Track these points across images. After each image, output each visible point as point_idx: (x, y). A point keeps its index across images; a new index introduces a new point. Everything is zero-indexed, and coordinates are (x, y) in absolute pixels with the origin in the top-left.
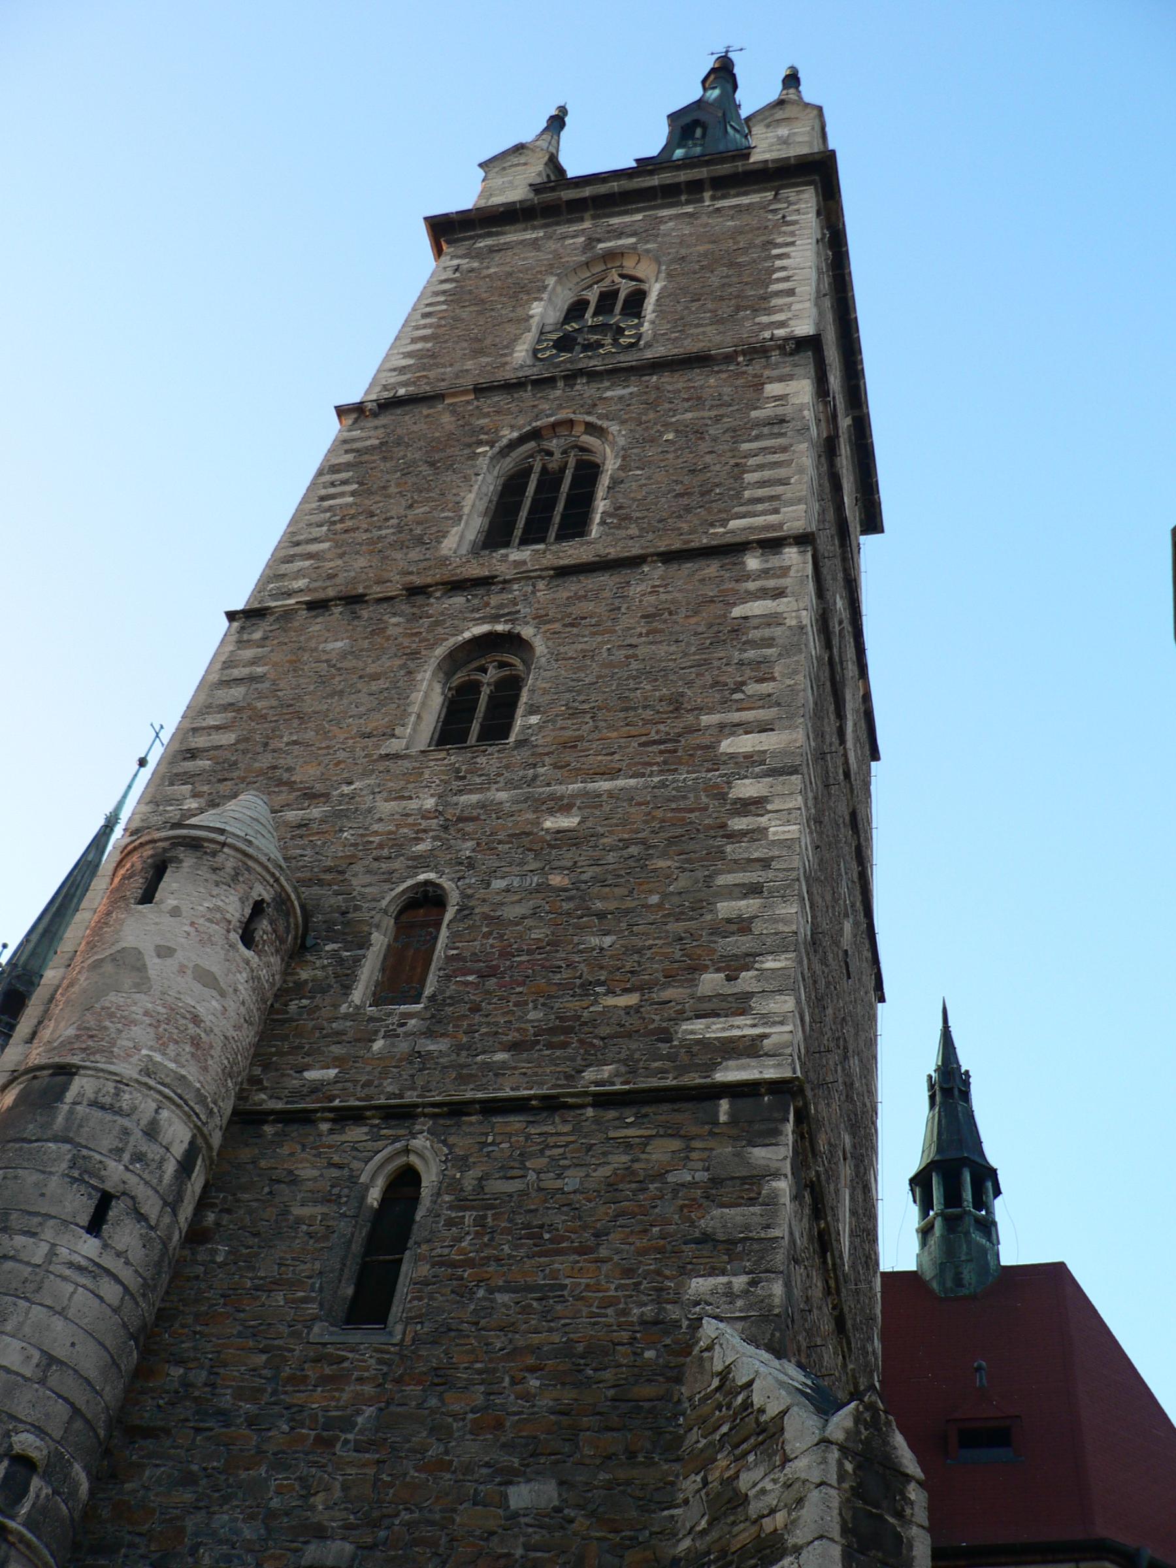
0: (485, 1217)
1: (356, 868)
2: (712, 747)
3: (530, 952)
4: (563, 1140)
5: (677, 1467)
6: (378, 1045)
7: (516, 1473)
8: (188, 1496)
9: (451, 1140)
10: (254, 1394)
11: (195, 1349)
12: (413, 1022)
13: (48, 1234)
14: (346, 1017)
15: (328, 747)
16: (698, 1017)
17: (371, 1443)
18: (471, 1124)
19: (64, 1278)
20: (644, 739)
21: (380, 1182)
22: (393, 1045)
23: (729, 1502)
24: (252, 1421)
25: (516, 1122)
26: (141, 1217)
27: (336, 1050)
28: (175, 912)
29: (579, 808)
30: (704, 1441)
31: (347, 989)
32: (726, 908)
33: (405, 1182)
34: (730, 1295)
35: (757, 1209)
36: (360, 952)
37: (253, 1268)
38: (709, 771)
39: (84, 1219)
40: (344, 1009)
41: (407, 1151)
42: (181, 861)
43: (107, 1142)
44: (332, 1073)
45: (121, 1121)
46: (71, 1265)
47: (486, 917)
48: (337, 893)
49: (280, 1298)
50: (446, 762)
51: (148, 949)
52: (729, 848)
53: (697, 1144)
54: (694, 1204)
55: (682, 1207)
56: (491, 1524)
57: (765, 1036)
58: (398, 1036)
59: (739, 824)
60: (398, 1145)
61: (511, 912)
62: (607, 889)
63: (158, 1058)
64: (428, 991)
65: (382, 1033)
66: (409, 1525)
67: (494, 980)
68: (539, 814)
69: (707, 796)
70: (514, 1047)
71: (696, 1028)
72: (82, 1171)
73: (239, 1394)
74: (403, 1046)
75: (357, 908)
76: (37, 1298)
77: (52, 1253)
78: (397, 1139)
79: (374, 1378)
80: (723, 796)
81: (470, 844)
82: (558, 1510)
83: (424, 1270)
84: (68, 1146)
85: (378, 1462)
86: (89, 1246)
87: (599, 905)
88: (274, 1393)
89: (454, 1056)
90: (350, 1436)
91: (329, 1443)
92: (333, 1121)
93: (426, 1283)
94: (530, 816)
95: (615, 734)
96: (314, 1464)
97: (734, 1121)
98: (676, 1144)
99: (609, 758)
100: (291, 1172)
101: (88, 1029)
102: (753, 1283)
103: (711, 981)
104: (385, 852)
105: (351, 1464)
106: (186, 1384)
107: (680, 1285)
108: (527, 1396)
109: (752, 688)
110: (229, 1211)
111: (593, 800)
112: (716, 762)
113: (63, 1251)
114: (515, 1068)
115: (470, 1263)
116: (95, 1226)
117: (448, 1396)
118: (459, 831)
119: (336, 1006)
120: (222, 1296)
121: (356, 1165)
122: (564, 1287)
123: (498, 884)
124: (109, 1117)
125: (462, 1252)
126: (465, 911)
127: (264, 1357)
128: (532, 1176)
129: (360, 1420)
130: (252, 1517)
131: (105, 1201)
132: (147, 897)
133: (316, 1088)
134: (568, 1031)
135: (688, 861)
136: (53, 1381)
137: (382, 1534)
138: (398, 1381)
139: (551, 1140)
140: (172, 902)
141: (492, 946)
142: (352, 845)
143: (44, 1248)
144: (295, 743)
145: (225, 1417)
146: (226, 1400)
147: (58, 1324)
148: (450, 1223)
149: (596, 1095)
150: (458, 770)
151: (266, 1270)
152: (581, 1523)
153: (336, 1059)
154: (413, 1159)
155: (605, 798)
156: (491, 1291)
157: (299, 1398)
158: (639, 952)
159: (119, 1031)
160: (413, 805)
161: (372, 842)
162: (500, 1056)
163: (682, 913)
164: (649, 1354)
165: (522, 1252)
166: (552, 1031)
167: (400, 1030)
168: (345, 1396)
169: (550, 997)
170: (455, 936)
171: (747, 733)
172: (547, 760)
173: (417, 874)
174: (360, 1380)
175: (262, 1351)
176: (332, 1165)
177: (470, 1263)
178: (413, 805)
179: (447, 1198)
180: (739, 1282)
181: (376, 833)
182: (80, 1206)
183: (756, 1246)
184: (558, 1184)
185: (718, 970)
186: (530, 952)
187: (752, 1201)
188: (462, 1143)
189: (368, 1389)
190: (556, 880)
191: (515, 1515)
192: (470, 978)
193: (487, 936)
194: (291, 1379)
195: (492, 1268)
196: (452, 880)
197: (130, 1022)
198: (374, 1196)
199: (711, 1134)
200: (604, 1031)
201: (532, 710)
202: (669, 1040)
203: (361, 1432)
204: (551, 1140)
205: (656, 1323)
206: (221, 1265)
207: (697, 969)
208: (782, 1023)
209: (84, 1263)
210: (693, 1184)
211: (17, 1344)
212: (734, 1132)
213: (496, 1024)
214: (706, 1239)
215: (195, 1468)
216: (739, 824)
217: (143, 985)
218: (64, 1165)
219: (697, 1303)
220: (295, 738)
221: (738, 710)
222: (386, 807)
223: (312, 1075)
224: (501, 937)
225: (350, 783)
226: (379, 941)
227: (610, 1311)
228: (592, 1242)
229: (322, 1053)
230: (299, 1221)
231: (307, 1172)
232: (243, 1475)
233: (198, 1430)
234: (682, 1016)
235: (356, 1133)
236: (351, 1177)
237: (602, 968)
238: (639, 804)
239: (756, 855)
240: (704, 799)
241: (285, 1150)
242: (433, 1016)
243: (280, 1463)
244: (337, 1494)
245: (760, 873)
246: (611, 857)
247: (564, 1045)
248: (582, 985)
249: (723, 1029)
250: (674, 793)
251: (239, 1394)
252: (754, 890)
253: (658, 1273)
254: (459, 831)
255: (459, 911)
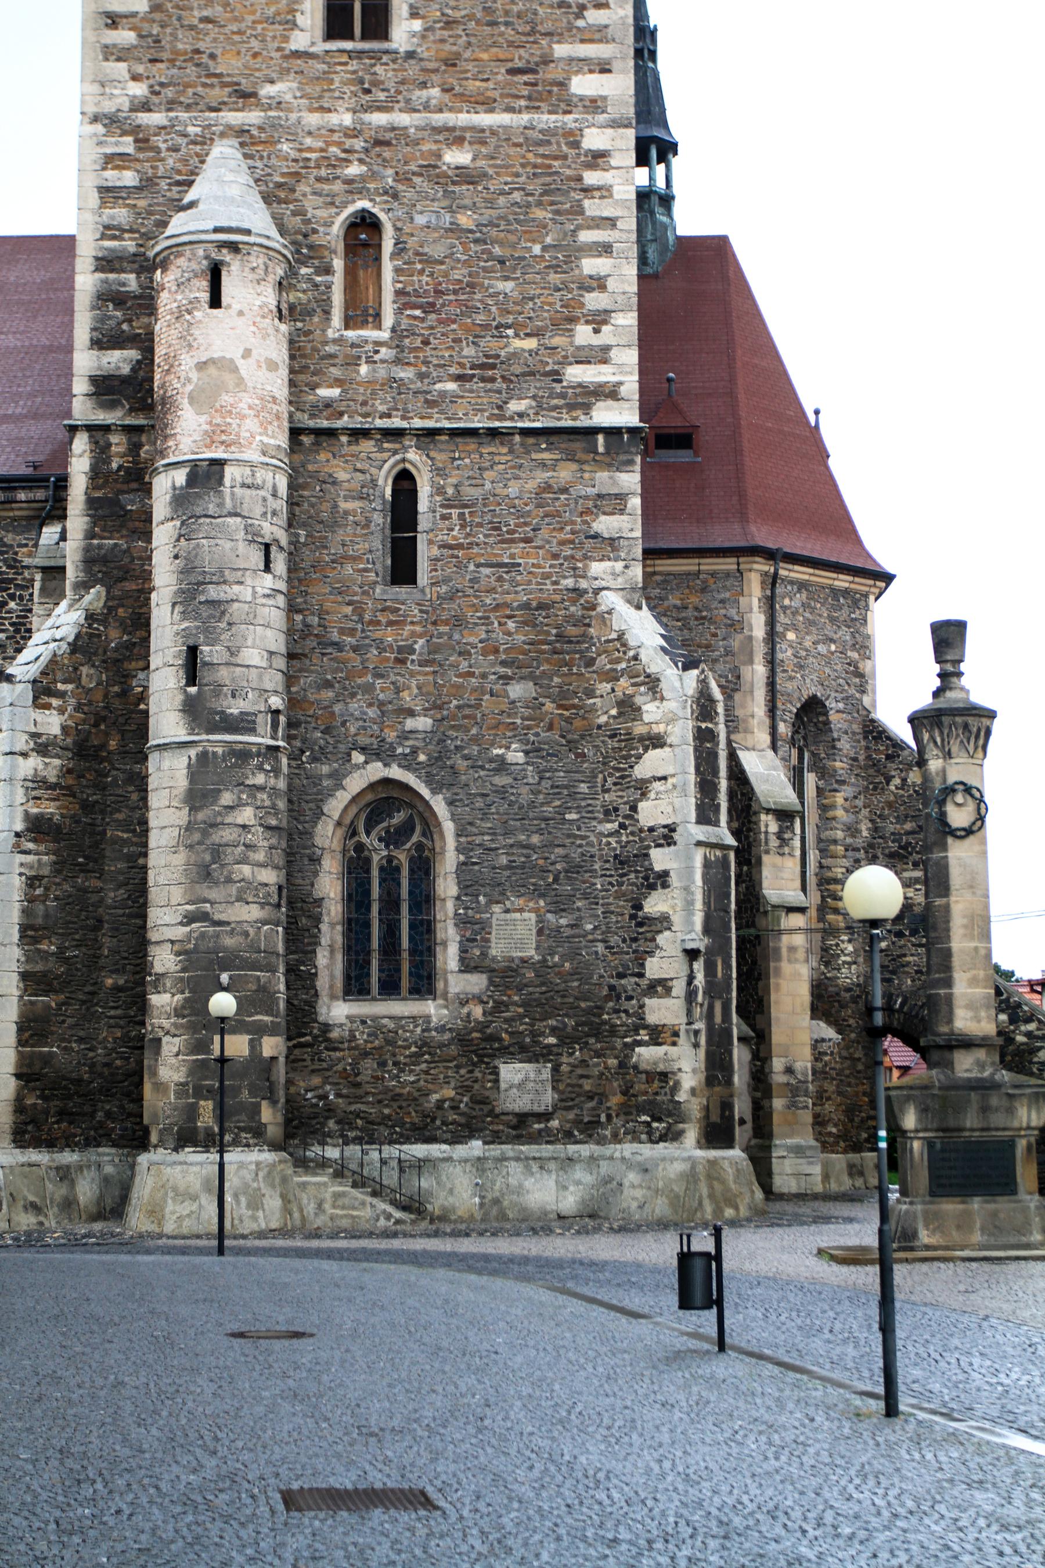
0: (463, 514)
1: (303, 188)
2: (563, 85)
3: (455, 292)
4: (503, 459)
5: (595, 676)
6: (364, 369)
7: (511, 678)
8: (330, 694)
9: (432, 454)
10: (352, 632)
11: (305, 602)
12: (383, 350)
13: (249, 581)
14: (335, 341)
15: (240, 33)
16: (577, 362)
17: (427, 661)
18: (442, 442)
19: (263, 605)
20: (510, 65)
21: (390, 482)
22: (374, 371)
23: (628, 708)
24: (355, 649)
25: (471, 444)
26: (281, 548)
27: (335, 372)
28: (241, 313)
29: (470, 143)
30: (608, 666)
31: (327, 313)
32: (590, 266)
33: (405, 480)
34: (615, 575)
35: (625, 517)
36: (328, 278)
37: (326, 547)
38: (566, 112)
39: (262, 566)
40: (331, 334)
41: (404, 460)
42: (229, 265)
43: (258, 511)
44: (335, 392)
45: (262, 493)
46: (264, 596)
47: (418, 254)
48: (294, 214)
49: (349, 569)
50: (349, 68)
51: (234, 353)
52: (587, 203)
53: (586, 467)
54: (587, 512)
55: (582, 513)
56: (504, 707)
57: (621, 383)
58: (375, 362)
59: (591, 178)
60: (398, 457)
61: (437, 251)
62: (502, 235)
63: (266, 440)
64: (388, 319)
65: (364, 359)
66: (458, 707)
67: (433, 316)
68: (439, 146)
69: (566, 144)
70: (459, 378)
71: (576, 374)
72: (253, 535)
73: (342, 631)
74: (382, 372)
75: (315, 231)
76: (255, 622)
77: (254, 593)
78: (395, 452)
79: (420, 622)
80: (576, 145)
81: (390, 172)
82: (536, 699)
83: (435, 551)
84: (239, 519)
85: (434, 672)
86: (268, 581)
87: (497, 250)
88: (363, 631)
89: (419, 384)
90: (414, 657)
91: (402, 662)
92: (350, 435)
93: (437, 560)
94: (434, 147)
95: (485, 56)
96: (399, 674)
97: (608, 452)
98: (574, 466)
99: (484, 84)
100: (330, 475)
101: (218, 425)
102: (626, 567)
103: (583, 334)
104: (323, 172)
105: (419, 673)
106: (307, 626)
107: (586, 566)
108: (509, 634)
109: (594, 17)
110: (298, 504)
111: (479, 136)
112: (568, 104)
113: (258, 589)
114: (462, 397)
115: (460, 547)
116: (267, 568)
117: (465, 632)
118: (379, 156)
119: (324, 331)
120: (313, 566)
121: (373, 471)
122: (519, 565)
123: (420, 220)
124: (254, 492)
125: (455, 538)
126: (400, 249)
127: (350, 608)
128: (488, 486)
129: (416, 647)
130: (370, 705)
131: (267, 546)
132: (215, 302)
133: (328, 404)
134: (493, 367)
135: (557, 212)
136: (274, 666)
137: (445, 713)
138: (434, 623)
139: (497, 459)
140: (236, 307)
141: (427, 284)
142: (294, 160)
143: (250, 589)
144: (206, 20)
145: (338, 646)
146: (335, 636)
147: (269, 633)
148: (444, 517)
149: (521, 429)
150: (361, 82)
151: (335, 549)
152: (549, 706)
153: (337, 380)
154: (408, 466)
155: (487, 134)
156: (478, 566)
157: (378, 634)
158: (532, 299)
159: (239, 426)
160: (334, 119)
161: (308, 160)
162: (451, 386)
163: (559, 266)
164: (573, 609)
165: (491, 540)
166: (483, 366)
167: (377, 357)
168: (405, 633)
169: (476, 336)
170: (398, 271)
171: (591, 71)
172: (435, 78)
173: (354, 201)
174: (412, 623)
175: (348, 604)
176: (356, 470)
177: (460, 547)
178: (334, 119)
179: (438, 498)
180: (619, 566)
181: (310, 149)
182: (256, 558)
183: (626, 543)
184: (505, 492)
185: (587, 322)
186: (455, 292)
187: (622, 512)
188: (441, 457)
189: (418, 629)
190: (465, 220)
191: (513, 702)
192: (418, 313)
193: (421, 272)
194: (371, 622)
195: (476, 550)
196: (383, 210)
197: (243, 417)
198: (388, 491)
199: (594, 460)
200: (518, 370)
201: (414, 14)
202: (560, 381)
203: (420, 654)
204: (497, 459)
205: (575, 590)
206: (305, 545)
207: (572, 320)
208: (631, 373)
209: (269, 592)
210: (586, 498)
211: (256, 651)
212: (608, 460)
213: (443, 357)
214: (596, 536)
215: (329, 677)
216: (591, 178)
217: (240, 382)
218: (242, 533)
219: (596, 579)
220: (205, 13)
221: (582, 41)
222: (313, 119)
223: (324, 392)
224: (432, 274)
225: (272, 82)
226: (338, 264)
227: (548, 582)
228: (531, 534)
229: (325, 374)
230: (346, 513)
231: (342, 475)
232: (359, 681)
233: (323, 654)
234: (565, 362)
235: (367, 446)
236: (372, 481)
237: (509, 313)
238: (516, 145)
239: (605, 214)
240: (564, 148)
241: (322, 457)
242: (398, 346)
243: (378, 675)
244: (416, 691)
245: (609, 232)
246: (502, 200)
247: (492, 380)
248: (497, 328)
249: (594, 375)
250: (541, 136)
251: (342, 631)
252: (606, 249)
253: (573, 557)
254: (379, 156)
255: (396, 244)
